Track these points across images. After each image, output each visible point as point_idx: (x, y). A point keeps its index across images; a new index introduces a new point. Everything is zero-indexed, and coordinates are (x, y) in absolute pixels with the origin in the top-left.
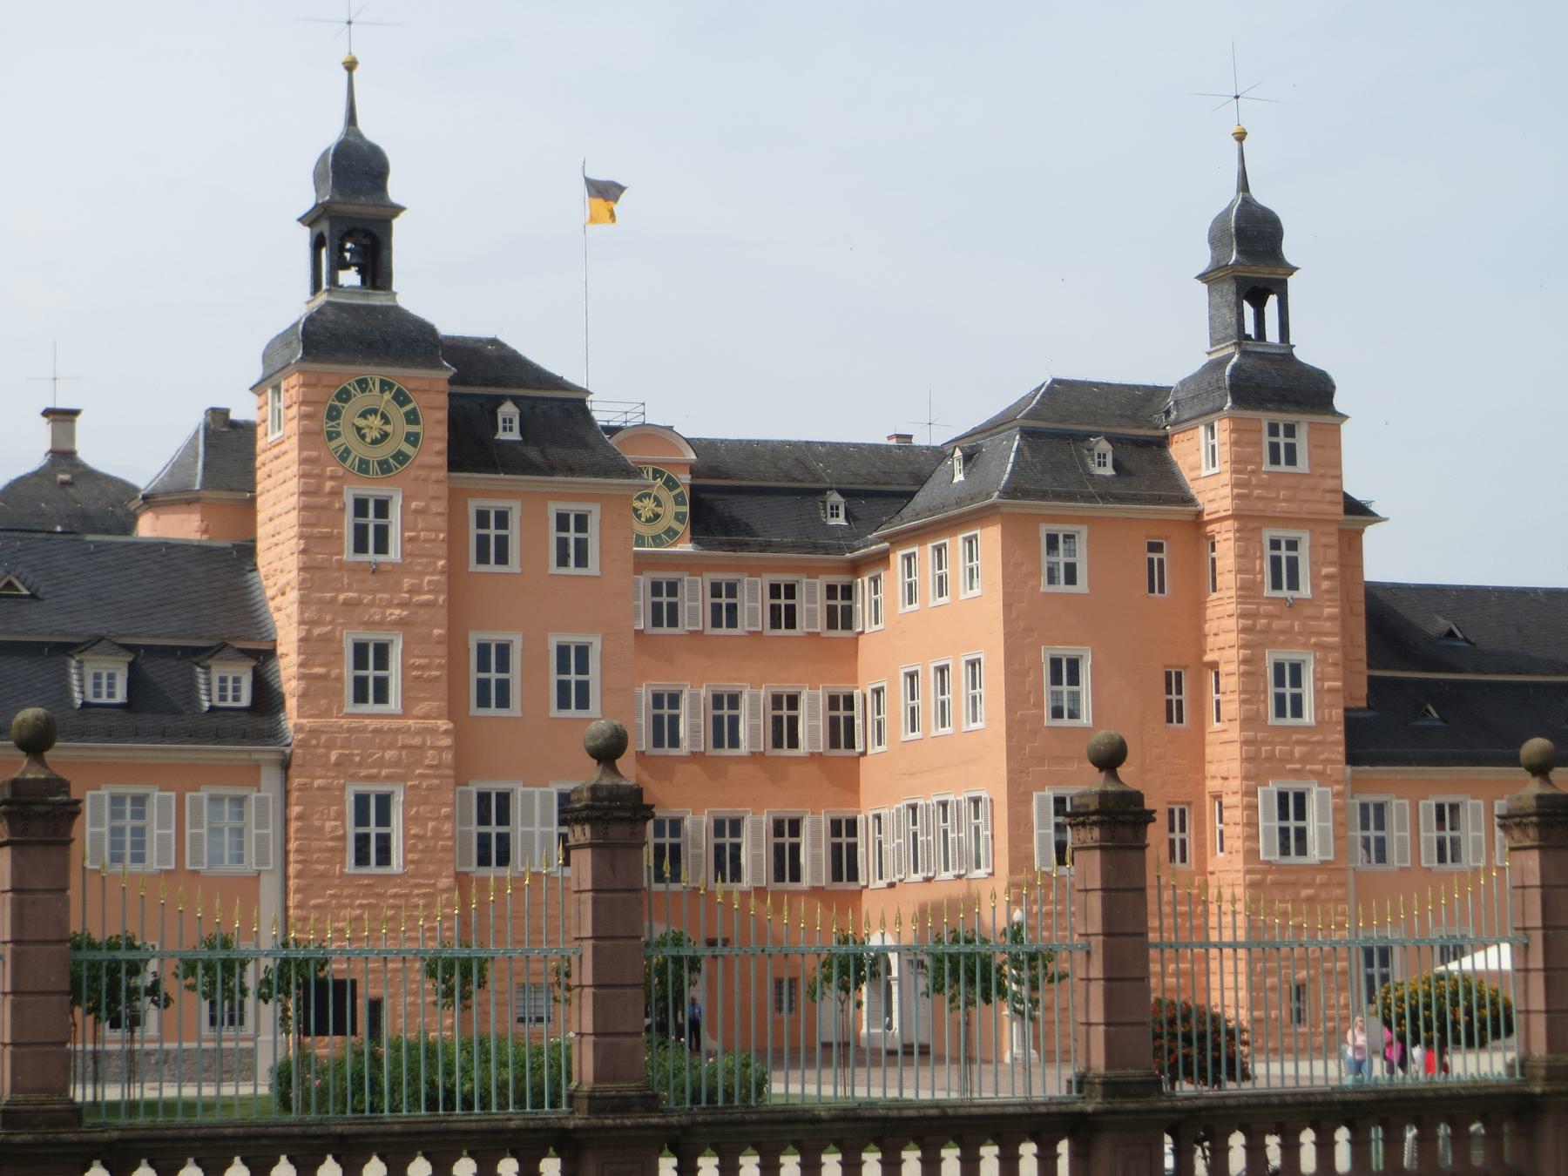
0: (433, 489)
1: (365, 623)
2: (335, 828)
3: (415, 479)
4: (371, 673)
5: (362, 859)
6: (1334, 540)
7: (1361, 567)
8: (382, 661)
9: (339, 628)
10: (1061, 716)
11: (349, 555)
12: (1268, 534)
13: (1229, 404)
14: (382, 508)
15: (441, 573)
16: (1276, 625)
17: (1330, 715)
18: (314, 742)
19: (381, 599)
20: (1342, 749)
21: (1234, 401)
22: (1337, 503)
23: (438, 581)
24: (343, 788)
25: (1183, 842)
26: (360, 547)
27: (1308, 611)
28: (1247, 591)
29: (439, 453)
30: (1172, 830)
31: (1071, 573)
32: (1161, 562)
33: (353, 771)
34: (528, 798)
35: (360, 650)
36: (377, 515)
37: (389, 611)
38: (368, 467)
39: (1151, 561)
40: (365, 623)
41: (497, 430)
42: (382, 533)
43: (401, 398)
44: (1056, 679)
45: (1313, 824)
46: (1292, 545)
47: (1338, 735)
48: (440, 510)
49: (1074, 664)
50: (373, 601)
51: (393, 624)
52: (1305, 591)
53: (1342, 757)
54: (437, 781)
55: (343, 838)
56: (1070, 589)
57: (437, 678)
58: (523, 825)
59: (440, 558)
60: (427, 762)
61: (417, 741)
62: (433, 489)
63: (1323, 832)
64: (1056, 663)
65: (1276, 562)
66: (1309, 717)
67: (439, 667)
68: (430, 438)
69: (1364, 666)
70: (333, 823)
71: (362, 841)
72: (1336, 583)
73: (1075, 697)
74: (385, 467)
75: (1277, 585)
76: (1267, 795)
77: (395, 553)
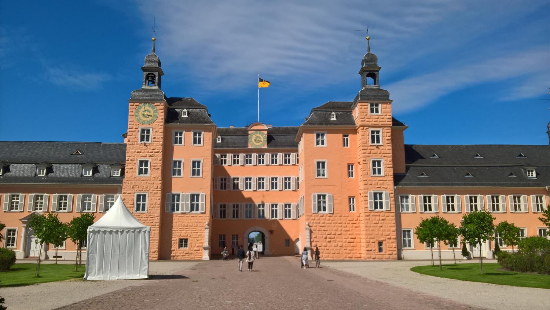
0: (160, 127)
1: (142, 157)
2: (131, 202)
3: (156, 125)
4: (143, 167)
5: (138, 209)
6: (390, 131)
7: (402, 138)
8: (146, 165)
9: (136, 158)
10: (320, 176)
11: (139, 142)
12: (370, 130)
13: (360, 99)
14: (148, 131)
15: (161, 145)
16: (372, 151)
17: (389, 174)
18: (127, 183)
19: (146, 151)
20: (393, 182)
21: (361, 99)
22: (390, 122)
23: (160, 147)
24: (134, 193)
25: (353, 206)
26: (142, 139)
27: (381, 148)
28: (365, 143)
29: (162, 119)
30: (350, 203)
31: (323, 143)
32: (347, 139)
33: (136, 189)
34: (183, 195)
35: (141, 163)
36: (147, 133)
37: (148, 154)
38: (145, 122)
39: (344, 139)
40: (142, 157)
41: (182, 115)
42: (148, 137)
43: (153, 108)
44: (318, 167)
45: (384, 200)
46: (378, 132)
47: (391, 178)
48: (162, 131)
49: (323, 163)
50: (144, 152)
51: (149, 157)
52: (381, 143)
53: (393, 184)
54: (157, 191)
55: (133, 204)
56: (323, 146)
57: (159, 168)
58: (177, 201)
59: (161, 142)
60: (154, 187)
61: (152, 182)
62: (160, 127)
63: (387, 203)
64: (318, 163)
65: (373, 137)
66: (382, 174)
67: (159, 166)
68: (160, 116)
69: (404, 162)
70: (132, 201)
71: (138, 206)
72: (390, 141)
73: (324, 171)
74: (149, 123)
75: (373, 141)
76: (370, 194)
77: (150, 142)
